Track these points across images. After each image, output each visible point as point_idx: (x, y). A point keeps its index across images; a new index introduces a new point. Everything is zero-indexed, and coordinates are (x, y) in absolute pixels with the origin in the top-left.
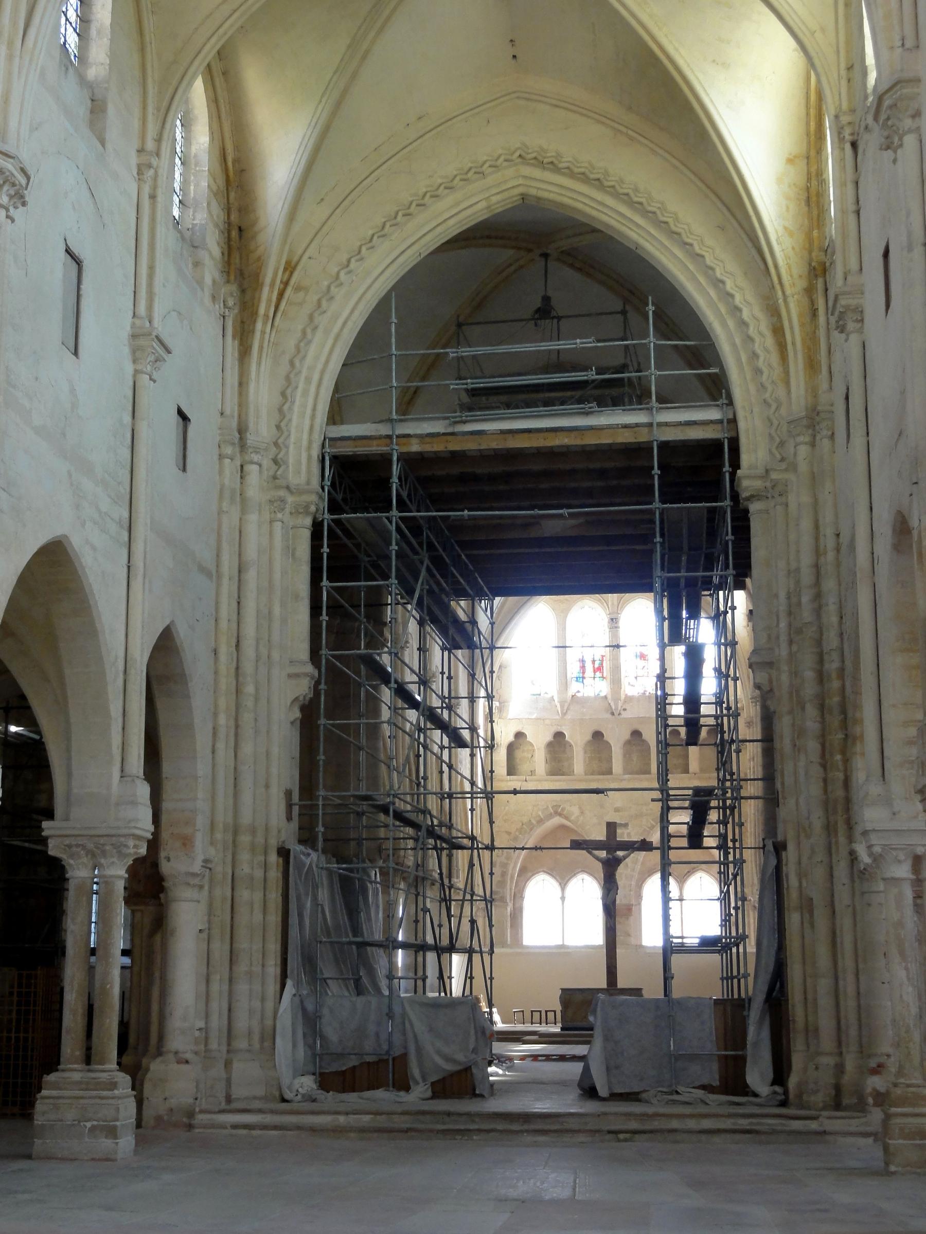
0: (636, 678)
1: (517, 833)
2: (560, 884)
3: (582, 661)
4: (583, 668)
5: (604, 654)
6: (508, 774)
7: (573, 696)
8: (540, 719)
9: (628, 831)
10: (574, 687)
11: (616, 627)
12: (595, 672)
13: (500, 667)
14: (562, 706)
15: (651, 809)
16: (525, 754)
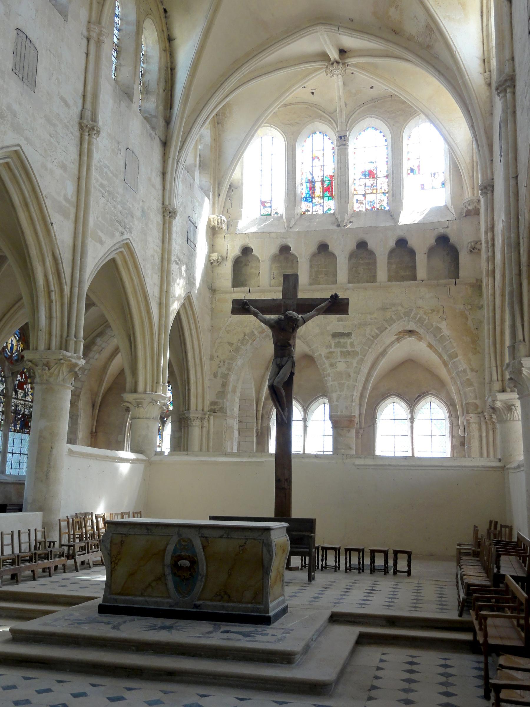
0: (364, 195)
1: (239, 344)
2: (303, 407)
3: (312, 182)
4: (312, 189)
5: (333, 174)
6: (234, 286)
7: (302, 215)
8: (266, 233)
9: (351, 340)
10: (304, 206)
11: (345, 145)
12: (324, 190)
13: (231, 187)
14: (289, 220)
15: (375, 318)
16: (253, 270)
